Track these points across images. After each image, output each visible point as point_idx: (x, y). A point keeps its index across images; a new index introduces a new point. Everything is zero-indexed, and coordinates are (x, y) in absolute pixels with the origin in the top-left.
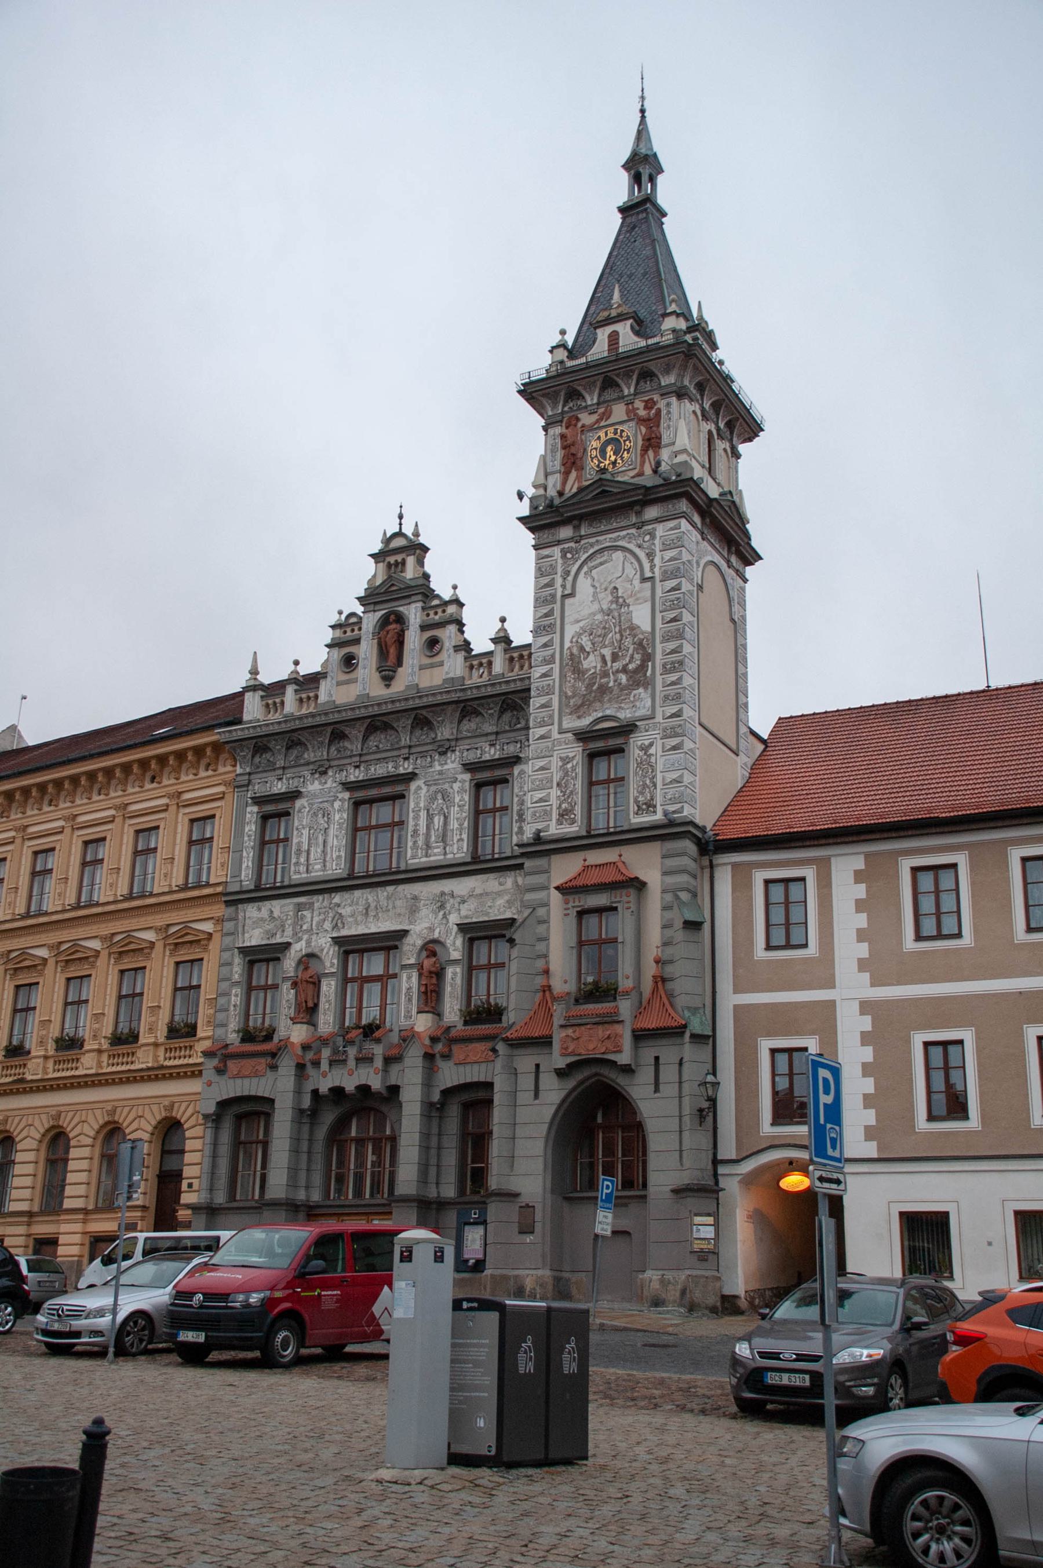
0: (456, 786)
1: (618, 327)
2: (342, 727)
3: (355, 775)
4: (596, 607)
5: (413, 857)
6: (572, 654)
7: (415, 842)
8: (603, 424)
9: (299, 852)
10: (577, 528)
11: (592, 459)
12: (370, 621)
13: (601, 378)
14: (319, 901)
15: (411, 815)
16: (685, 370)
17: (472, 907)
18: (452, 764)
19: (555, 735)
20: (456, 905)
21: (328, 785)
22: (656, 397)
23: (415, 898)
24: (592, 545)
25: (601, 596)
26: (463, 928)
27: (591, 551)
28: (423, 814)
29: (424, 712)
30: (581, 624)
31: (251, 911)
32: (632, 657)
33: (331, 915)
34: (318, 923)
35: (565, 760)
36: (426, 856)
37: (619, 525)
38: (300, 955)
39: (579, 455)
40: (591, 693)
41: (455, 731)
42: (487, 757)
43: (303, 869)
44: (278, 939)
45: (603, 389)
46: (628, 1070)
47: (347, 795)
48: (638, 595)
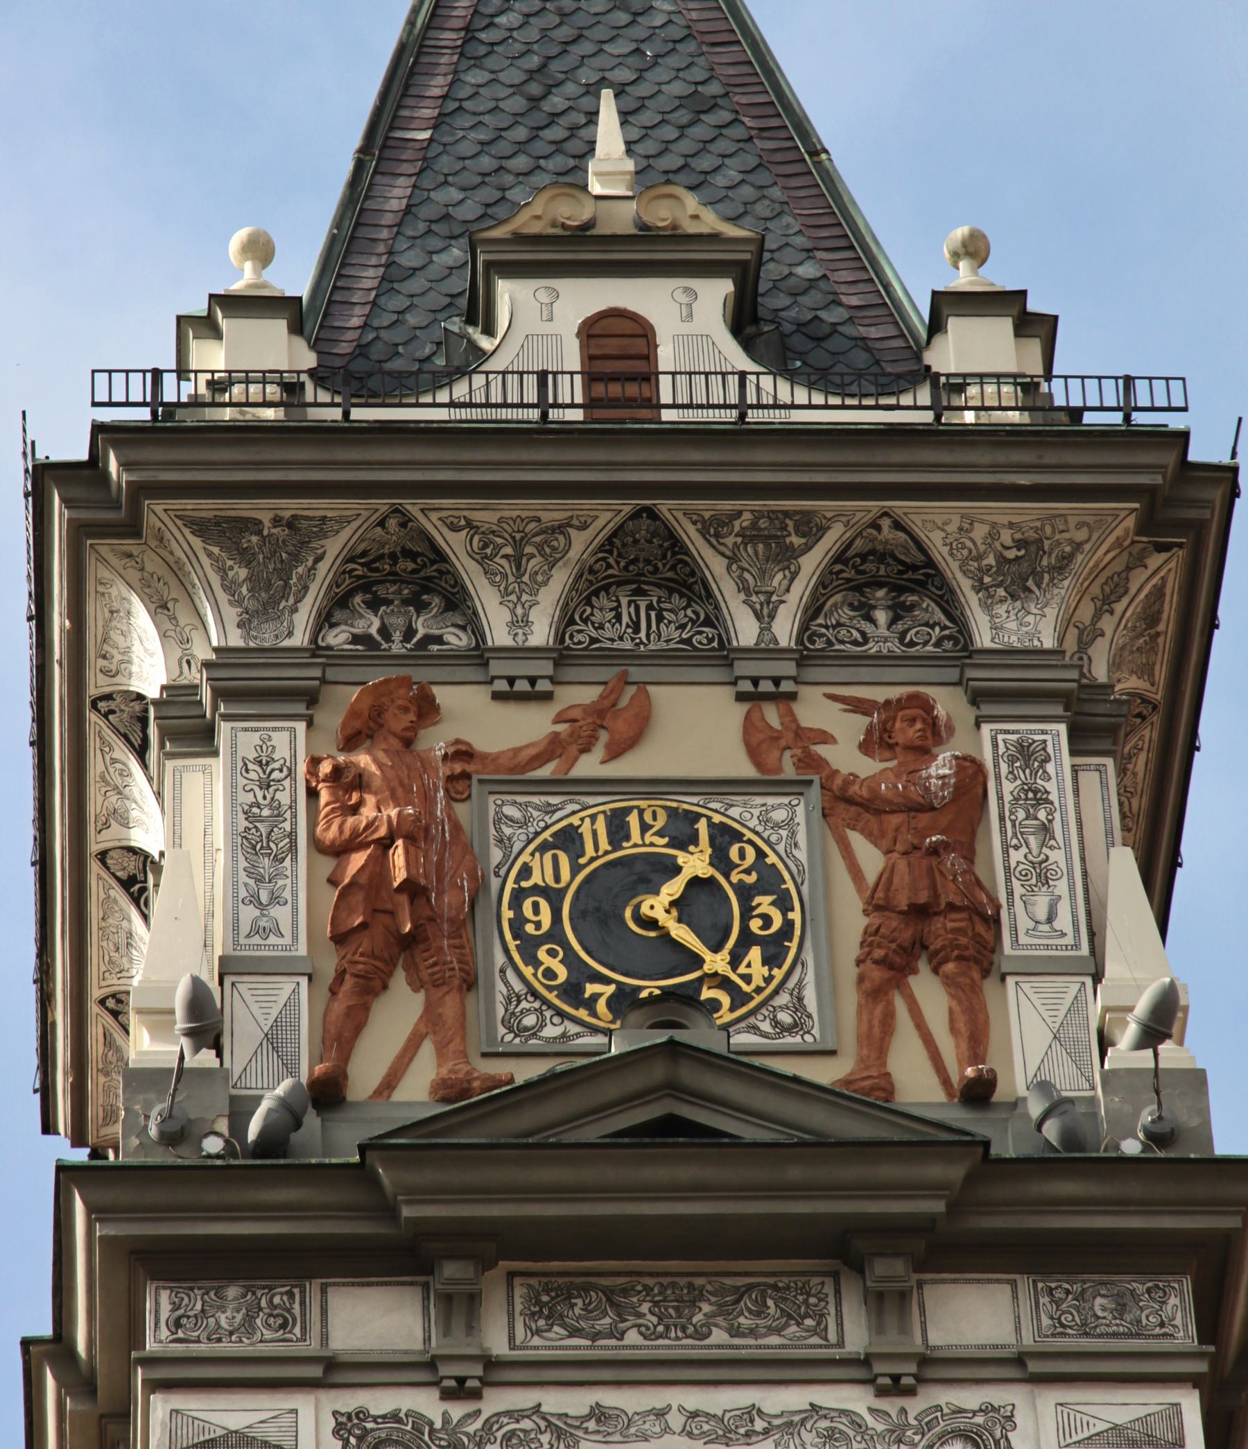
1: (651, 299)
8: (589, 766)
10: (458, 1307)
11: (529, 947)
13: (605, 515)
16: (1105, 604)
22: (948, 703)
37: (747, 1347)
39: (448, 902)
45: (590, 588)
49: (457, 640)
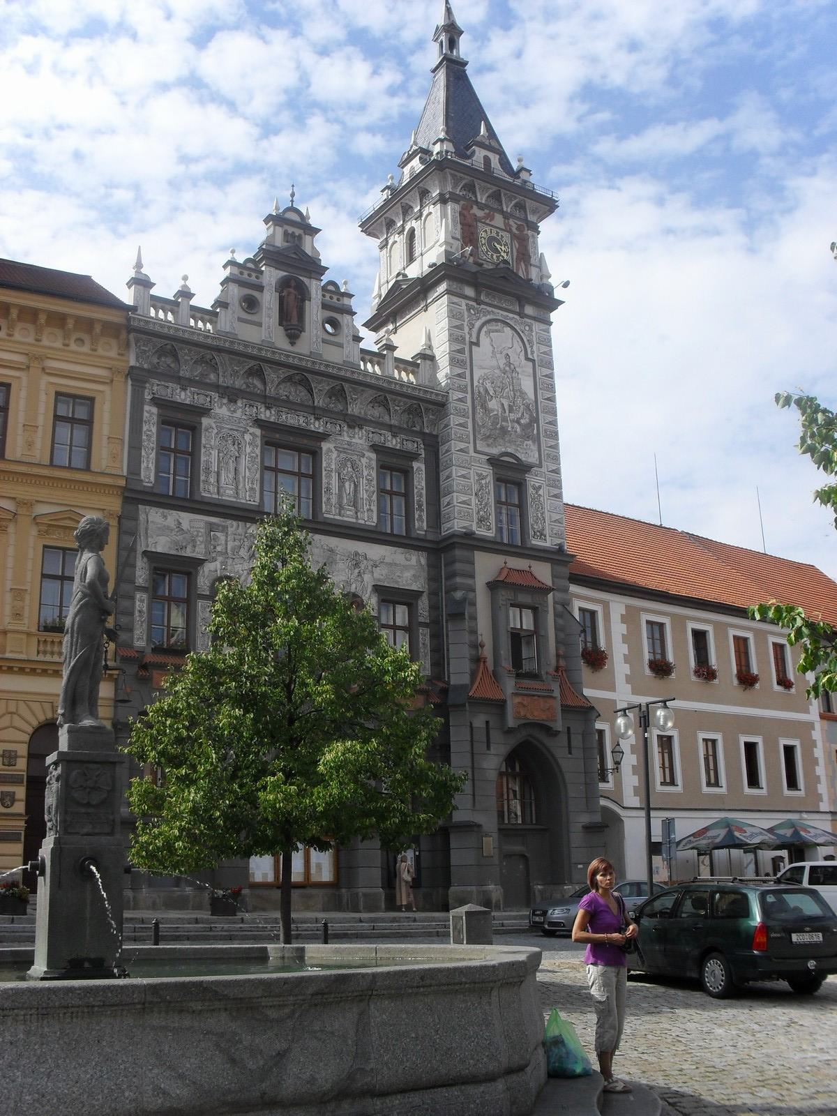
0: (364, 461)
2: (265, 366)
3: (267, 415)
4: (494, 363)
5: (329, 512)
6: (479, 392)
7: (328, 499)
9: (208, 469)
10: (478, 292)
12: (271, 275)
13: (495, 188)
14: (232, 525)
15: (324, 473)
17: (384, 573)
18: (359, 439)
19: (472, 453)
20: (370, 568)
21: (238, 414)
23: (331, 550)
24: (489, 312)
25: (498, 356)
26: (377, 589)
27: (489, 317)
28: (335, 476)
29: (346, 386)
30: (486, 371)
31: (153, 517)
32: (523, 414)
33: (246, 543)
34: (233, 549)
35: (481, 477)
36: (340, 515)
38: (214, 576)
40: (495, 429)
41: (363, 412)
42: (389, 445)
43: (213, 489)
44: (188, 553)
46: (556, 734)
47: (258, 432)
48: (524, 369)
49: (474, 199)
